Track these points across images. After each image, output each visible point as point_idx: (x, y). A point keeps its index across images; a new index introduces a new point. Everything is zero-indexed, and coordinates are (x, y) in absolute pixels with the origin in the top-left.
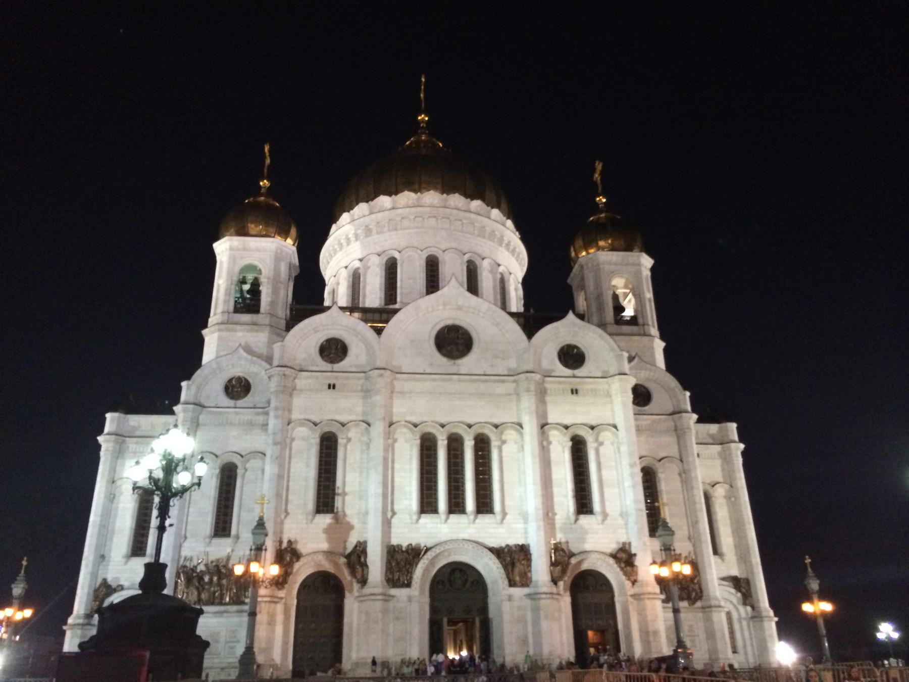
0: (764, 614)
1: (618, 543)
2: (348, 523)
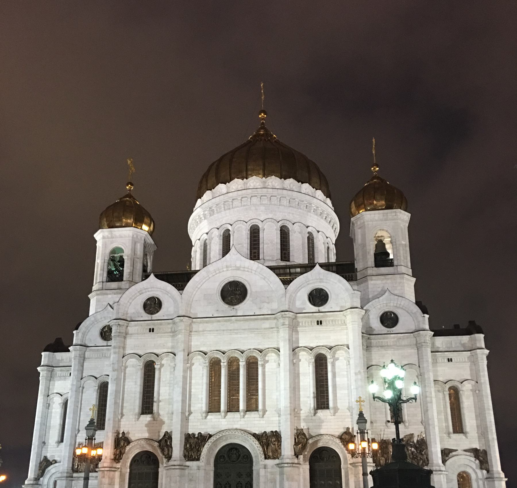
0: (496, 475)
1: (344, 428)
2: (161, 420)
